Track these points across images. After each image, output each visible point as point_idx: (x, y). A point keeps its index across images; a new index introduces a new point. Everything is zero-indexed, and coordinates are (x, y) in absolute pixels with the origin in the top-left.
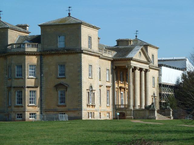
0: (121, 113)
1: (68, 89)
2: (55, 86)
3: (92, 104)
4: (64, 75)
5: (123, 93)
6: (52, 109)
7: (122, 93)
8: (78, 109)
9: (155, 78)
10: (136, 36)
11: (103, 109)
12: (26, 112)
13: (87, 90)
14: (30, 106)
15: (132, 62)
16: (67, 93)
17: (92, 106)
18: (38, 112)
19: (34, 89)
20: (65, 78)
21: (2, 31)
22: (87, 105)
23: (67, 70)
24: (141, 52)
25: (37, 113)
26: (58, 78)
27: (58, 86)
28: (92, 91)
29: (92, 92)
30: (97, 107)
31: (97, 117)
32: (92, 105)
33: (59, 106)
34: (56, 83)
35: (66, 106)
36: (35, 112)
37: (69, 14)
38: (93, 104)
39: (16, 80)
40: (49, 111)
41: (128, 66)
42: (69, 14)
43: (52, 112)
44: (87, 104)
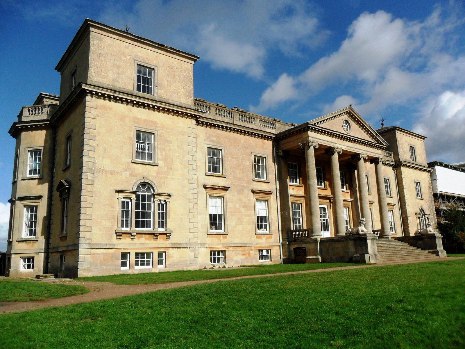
0: (297, 247)
5: (326, 207)
7: (324, 209)
9: (421, 183)
10: (382, 124)
11: (237, 241)
12: (13, 256)
15: (310, 133)
18: (38, 253)
19: (34, 201)
22: (119, 235)
24: (349, 120)
25: (36, 256)
28: (154, 195)
31: (235, 260)
36: (32, 255)
41: (303, 144)
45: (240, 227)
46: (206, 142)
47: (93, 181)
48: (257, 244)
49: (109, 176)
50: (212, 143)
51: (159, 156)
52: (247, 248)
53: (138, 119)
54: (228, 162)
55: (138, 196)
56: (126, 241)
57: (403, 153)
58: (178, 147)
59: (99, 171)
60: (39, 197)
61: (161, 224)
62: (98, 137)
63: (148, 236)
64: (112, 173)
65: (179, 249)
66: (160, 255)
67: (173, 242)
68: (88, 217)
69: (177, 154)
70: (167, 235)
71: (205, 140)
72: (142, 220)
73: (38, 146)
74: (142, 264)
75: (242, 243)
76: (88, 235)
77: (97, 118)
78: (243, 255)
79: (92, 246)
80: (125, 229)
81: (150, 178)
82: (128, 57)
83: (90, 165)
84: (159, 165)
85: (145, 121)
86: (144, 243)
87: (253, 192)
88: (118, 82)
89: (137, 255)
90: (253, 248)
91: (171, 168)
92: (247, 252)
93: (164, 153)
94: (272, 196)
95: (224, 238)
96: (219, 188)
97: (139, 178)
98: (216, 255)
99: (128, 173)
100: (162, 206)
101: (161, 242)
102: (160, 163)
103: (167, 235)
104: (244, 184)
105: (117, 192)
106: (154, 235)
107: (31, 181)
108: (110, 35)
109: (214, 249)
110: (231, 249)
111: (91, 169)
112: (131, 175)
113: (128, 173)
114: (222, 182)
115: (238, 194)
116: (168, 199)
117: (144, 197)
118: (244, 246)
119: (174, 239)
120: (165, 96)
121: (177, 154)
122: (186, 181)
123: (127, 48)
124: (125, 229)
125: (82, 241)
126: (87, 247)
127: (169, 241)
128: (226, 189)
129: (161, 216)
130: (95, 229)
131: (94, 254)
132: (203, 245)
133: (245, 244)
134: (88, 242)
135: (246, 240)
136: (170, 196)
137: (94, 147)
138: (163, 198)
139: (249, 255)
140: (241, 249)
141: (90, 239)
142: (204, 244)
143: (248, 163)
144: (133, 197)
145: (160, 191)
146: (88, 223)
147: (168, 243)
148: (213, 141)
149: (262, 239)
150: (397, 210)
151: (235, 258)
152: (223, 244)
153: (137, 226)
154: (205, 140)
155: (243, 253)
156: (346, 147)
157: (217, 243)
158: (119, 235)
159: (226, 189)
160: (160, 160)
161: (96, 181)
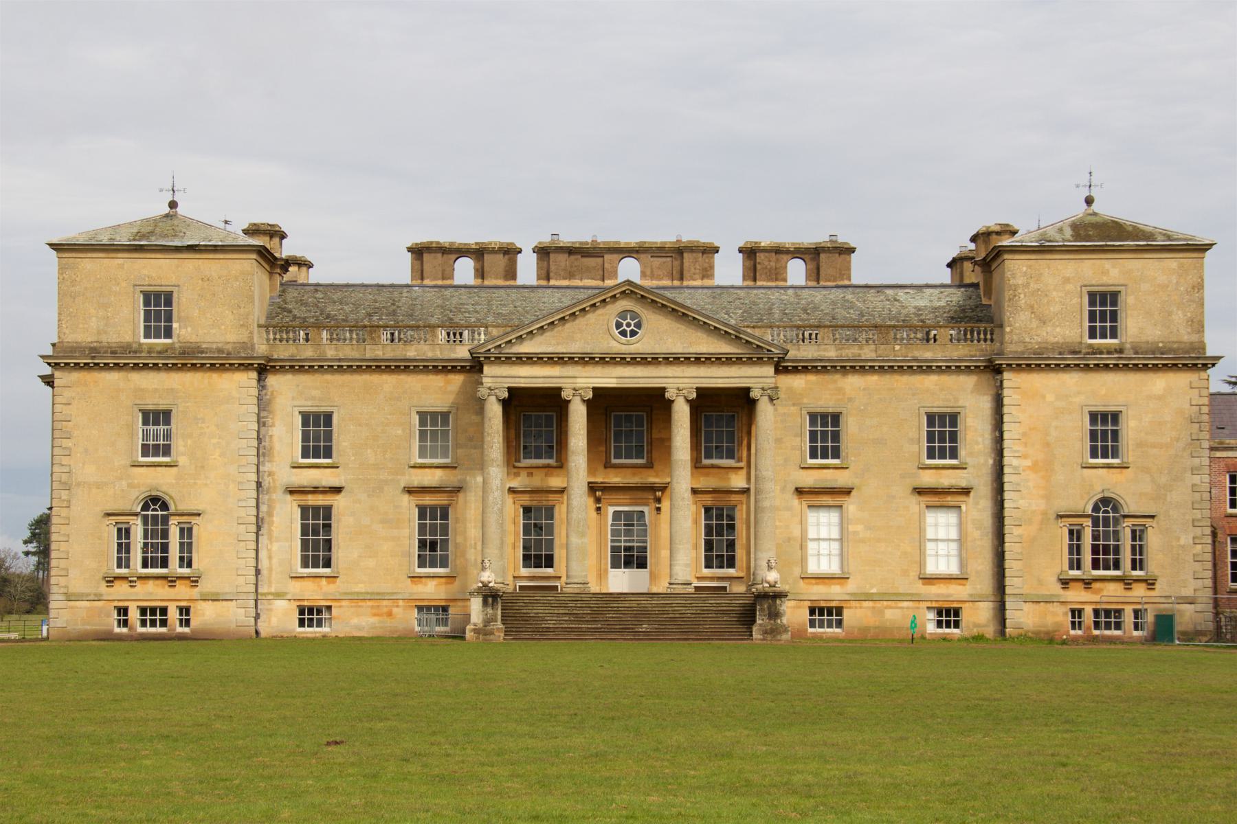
10: (1089, 201)
11: (361, 588)
24: (637, 308)
37: (173, 205)
42: (173, 205)
45: (371, 563)
46: (296, 403)
47: (69, 501)
48: (411, 594)
49: (94, 491)
50: (310, 403)
51: (182, 449)
52: (385, 603)
53: (142, 390)
54: (343, 437)
55: (145, 518)
56: (121, 589)
57: (1035, 324)
58: (217, 426)
59: (78, 484)
61: (186, 562)
62: (76, 433)
63: (159, 582)
64: (99, 486)
66: (185, 611)
67: (206, 590)
68: (62, 555)
69: (214, 441)
70: (194, 581)
71: (293, 399)
72: (156, 556)
74: (153, 623)
75: (372, 594)
76: (62, 581)
78: (375, 615)
79: (69, 597)
80: (123, 571)
81: (164, 489)
82: (124, 284)
83: (64, 477)
84: (180, 464)
85: (156, 390)
86: (154, 593)
87: (410, 491)
88: (106, 332)
89: (143, 611)
90: (401, 603)
91: (203, 467)
92: (385, 610)
93: (189, 442)
94: (461, 495)
96: (315, 490)
97: (143, 489)
98: (310, 614)
99: (124, 483)
100: (187, 532)
101: (182, 591)
102: (182, 460)
103: (194, 581)
104: (384, 476)
105: (109, 515)
106: (171, 580)
108: (89, 255)
109: (306, 603)
110: (344, 603)
111: (65, 483)
112: (129, 485)
113: (124, 483)
114: (326, 478)
115: (369, 496)
116: (194, 520)
117: (155, 517)
118: (376, 597)
119: (206, 586)
120: (194, 339)
121: (214, 441)
123: (121, 267)
124: (123, 571)
125: (54, 589)
126: (61, 597)
127: (196, 590)
128: (337, 490)
129: (187, 547)
130: (73, 573)
131: (72, 608)
132: (279, 596)
133: (378, 594)
134: (63, 590)
135: (385, 587)
137: (70, 449)
139: (390, 614)
140: (370, 603)
141: (66, 587)
142: (286, 593)
143: (400, 432)
144: (139, 521)
145: (182, 507)
146: (63, 564)
147: (195, 593)
148: (313, 398)
149: (426, 585)
150: (979, 508)
151: (355, 621)
153: (145, 565)
154: (293, 399)
155: (374, 611)
156: (614, 380)
157: (313, 592)
158: (111, 580)
159: (337, 490)
160: (183, 454)
161: (73, 502)
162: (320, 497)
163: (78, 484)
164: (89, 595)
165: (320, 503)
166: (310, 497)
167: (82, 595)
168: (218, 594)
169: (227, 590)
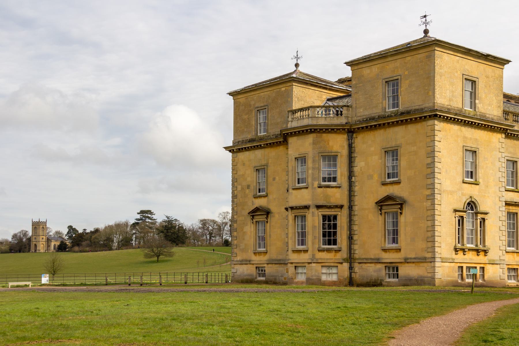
1: (404, 210)
2: (376, 203)
3: (477, 246)
4: (395, 175)
6: (373, 257)
8: (425, 258)
13: (456, 211)
14: (323, 250)
16: (402, 219)
17: (475, 253)
19: (333, 210)
20: (398, 183)
21: (283, 89)
22: (456, 250)
23: (403, 162)
26: (384, 184)
27: (383, 203)
28: (477, 213)
29: (477, 216)
30: (493, 255)
32: (477, 248)
33: (385, 250)
34: (380, 198)
35: (400, 250)
38: (481, 247)
39: (294, 192)
40: (366, 263)
43: (373, 265)
44: (455, 246)
49: (450, 196)
59: (444, 191)
60: (341, 207)
62: (443, 160)
64: (451, 193)
65: (493, 265)
69: (491, 172)
73: (333, 151)
77: (442, 141)
91: (487, 186)
95: (517, 256)
101: (482, 258)
103: (486, 252)
106: (478, 251)
107: (328, 189)
112: (462, 194)
122: (497, 199)
127: (486, 257)
130: (443, 245)
136: (486, 214)
138: (483, 216)
152: (517, 262)
162: (514, 208)
163: (444, 191)
164: (449, 259)
165: (514, 211)
166: (511, 207)
167: (447, 259)
168: (494, 260)
169: (497, 258)
